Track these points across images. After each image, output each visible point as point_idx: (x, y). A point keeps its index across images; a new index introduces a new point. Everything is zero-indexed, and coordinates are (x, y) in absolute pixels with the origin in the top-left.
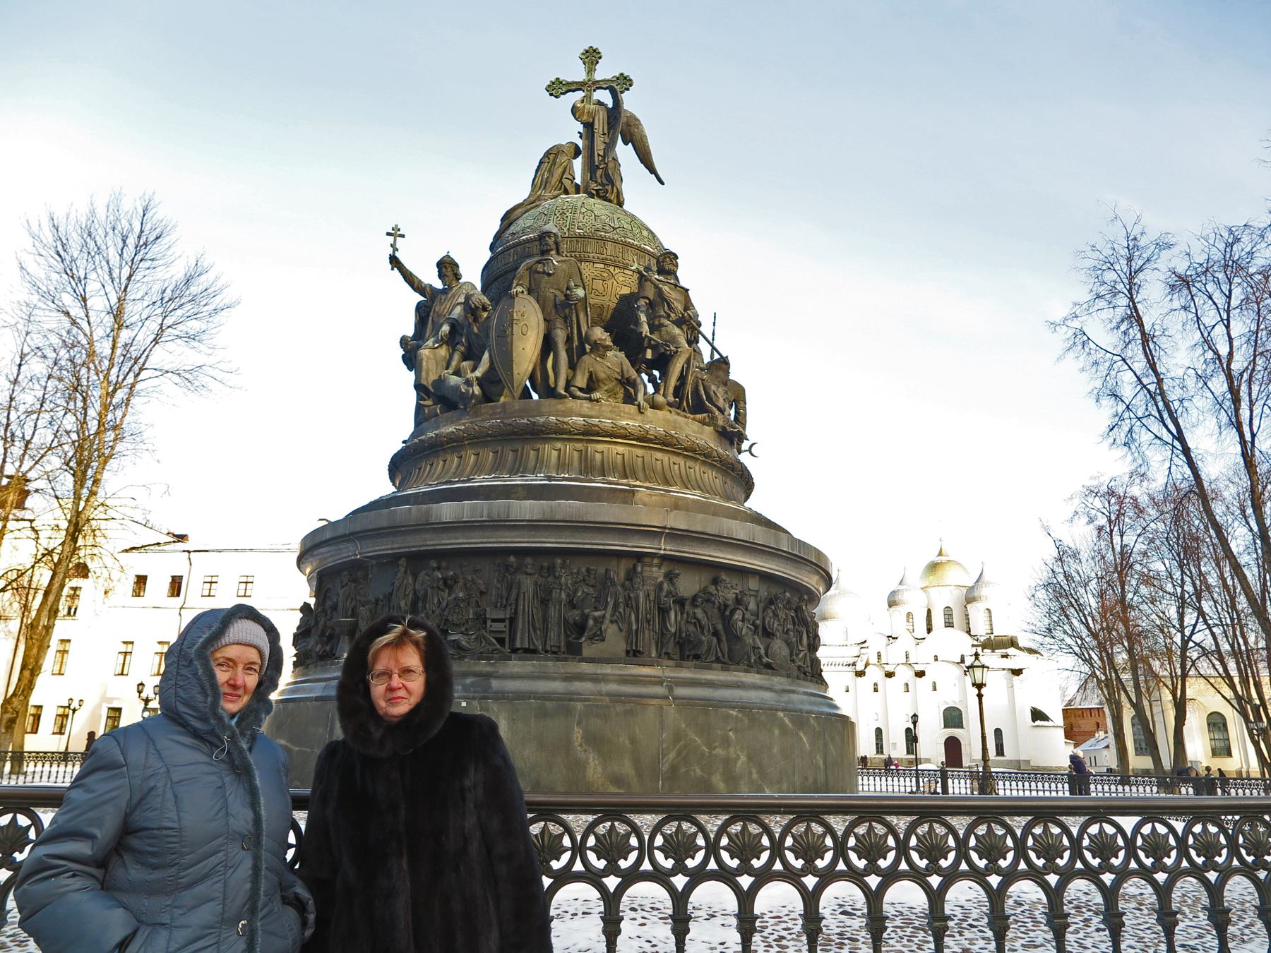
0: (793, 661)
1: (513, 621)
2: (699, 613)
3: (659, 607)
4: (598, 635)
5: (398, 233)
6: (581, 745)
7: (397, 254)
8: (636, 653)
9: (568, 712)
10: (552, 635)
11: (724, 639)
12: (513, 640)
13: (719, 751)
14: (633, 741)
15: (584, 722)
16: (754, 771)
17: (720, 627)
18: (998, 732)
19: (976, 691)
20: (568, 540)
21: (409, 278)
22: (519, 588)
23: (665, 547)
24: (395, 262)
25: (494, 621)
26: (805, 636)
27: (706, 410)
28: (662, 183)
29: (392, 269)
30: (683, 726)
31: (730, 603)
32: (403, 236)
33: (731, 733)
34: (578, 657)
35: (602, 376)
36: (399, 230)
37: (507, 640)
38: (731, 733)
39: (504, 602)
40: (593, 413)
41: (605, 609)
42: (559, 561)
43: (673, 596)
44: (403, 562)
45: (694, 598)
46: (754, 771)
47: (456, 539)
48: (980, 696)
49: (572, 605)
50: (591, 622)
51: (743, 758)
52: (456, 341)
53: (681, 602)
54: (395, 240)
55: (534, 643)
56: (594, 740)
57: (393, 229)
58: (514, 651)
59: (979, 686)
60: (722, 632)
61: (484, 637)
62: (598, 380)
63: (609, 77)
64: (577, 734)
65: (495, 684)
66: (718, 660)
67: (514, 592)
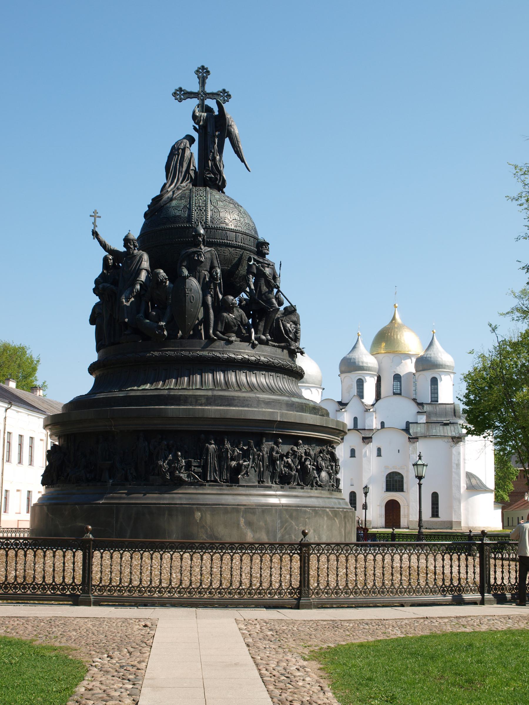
5: (97, 215)
6: (243, 526)
7: (97, 229)
15: (245, 516)
18: (435, 497)
19: (417, 481)
24: (95, 234)
25: (195, 466)
26: (334, 467)
29: (94, 239)
30: (287, 516)
31: (303, 455)
32: (100, 217)
33: (307, 520)
34: (237, 485)
36: (97, 213)
38: (307, 520)
41: (249, 461)
43: (278, 453)
48: (420, 485)
49: (232, 459)
56: (249, 524)
57: (94, 212)
59: (420, 478)
63: (215, 91)
64: (242, 521)
66: (298, 484)
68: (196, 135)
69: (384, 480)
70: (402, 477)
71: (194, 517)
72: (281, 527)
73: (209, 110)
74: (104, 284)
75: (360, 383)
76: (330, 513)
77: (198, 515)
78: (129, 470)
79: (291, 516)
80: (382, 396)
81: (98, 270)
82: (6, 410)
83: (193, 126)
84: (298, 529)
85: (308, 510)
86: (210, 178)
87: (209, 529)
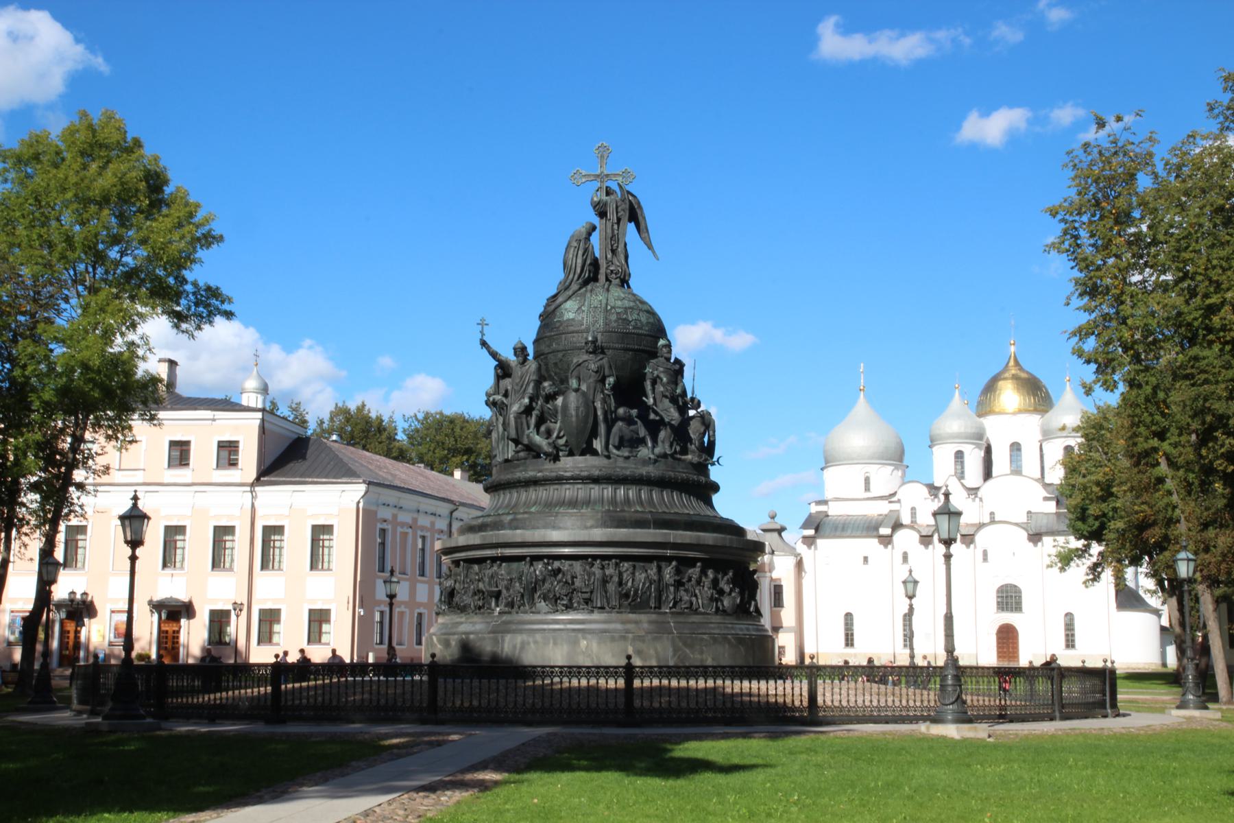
7: (485, 338)
11: (699, 597)
13: (698, 656)
14: (657, 652)
23: (669, 552)
24: (484, 344)
28: (658, 259)
30: (680, 644)
35: (626, 438)
44: (528, 559)
54: (482, 328)
67: (593, 578)
68: (596, 220)
69: (994, 595)
70: (1020, 592)
72: (674, 655)
73: (609, 192)
74: (494, 396)
75: (959, 455)
76: (733, 640)
77: (584, 643)
79: (685, 644)
80: (994, 474)
81: (489, 380)
82: (451, 513)
86: (612, 271)
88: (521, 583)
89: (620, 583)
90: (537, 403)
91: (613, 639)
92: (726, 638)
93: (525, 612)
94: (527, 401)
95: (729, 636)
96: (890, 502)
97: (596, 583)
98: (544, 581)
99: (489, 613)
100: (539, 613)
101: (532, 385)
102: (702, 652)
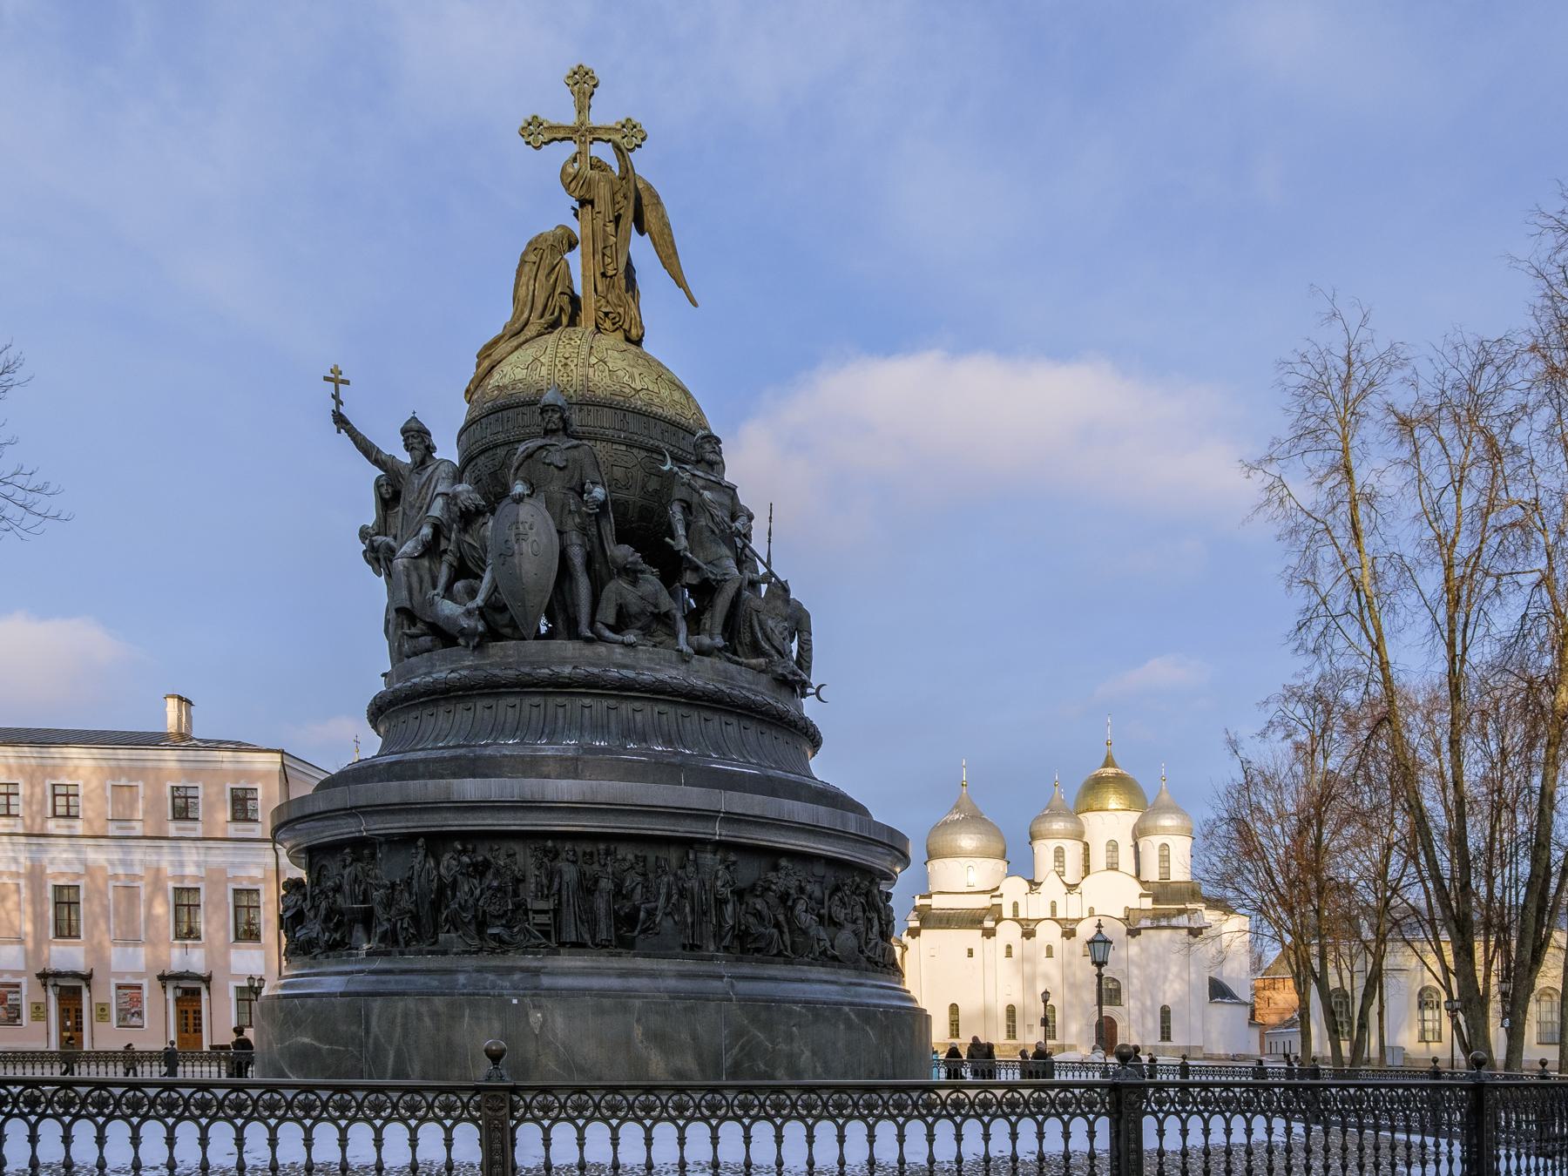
0: (862, 952)
1: (556, 912)
2: (759, 905)
3: (715, 898)
4: (652, 929)
6: (642, 1042)
8: (693, 947)
9: (626, 1009)
10: (603, 925)
11: (786, 930)
12: (559, 932)
13: (783, 1047)
14: (695, 1038)
15: (644, 1020)
16: (818, 1065)
17: (781, 918)
20: (612, 825)
21: (367, 449)
22: (561, 877)
23: (718, 832)
26: (876, 922)
27: (763, 654)
30: (746, 1022)
31: (792, 891)
37: (553, 933)
38: (794, 1029)
39: (546, 892)
40: (628, 661)
42: (602, 847)
43: (731, 886)
44: (421, 842)
45: (753, 888)
46: (818, 1065)
47: (484, 819)
50: (642, 915)
51: (807, 1053)
52: (442, 548)
53: (740, 894)
55: (582, 937)
58: (562, 944)
60: (784, 923)
61: (528, 930)
62: (630, 616)
65: (546, 981)
66: (779, 954)
67: (557, 880)
71: (528, 1022)
76: (853, 1016)
78: (399, 925)
83: (573, 208)
84: (773, 1048)
85: (797, 1008)
87: (561, 1048)
88: (410, 894)
89: (619, 893)
90: (449, 540)
91: (600, 1011)
92: (839, 1010)
93: (419, 953)
94: (426, 531)
95: (846, 1009)
96: (992, 897)
97: (564, 893)
98: (454, 885)
99: (350, 955)
100: (445, 953)
101: (439, 502)
102: (790, 1038)
